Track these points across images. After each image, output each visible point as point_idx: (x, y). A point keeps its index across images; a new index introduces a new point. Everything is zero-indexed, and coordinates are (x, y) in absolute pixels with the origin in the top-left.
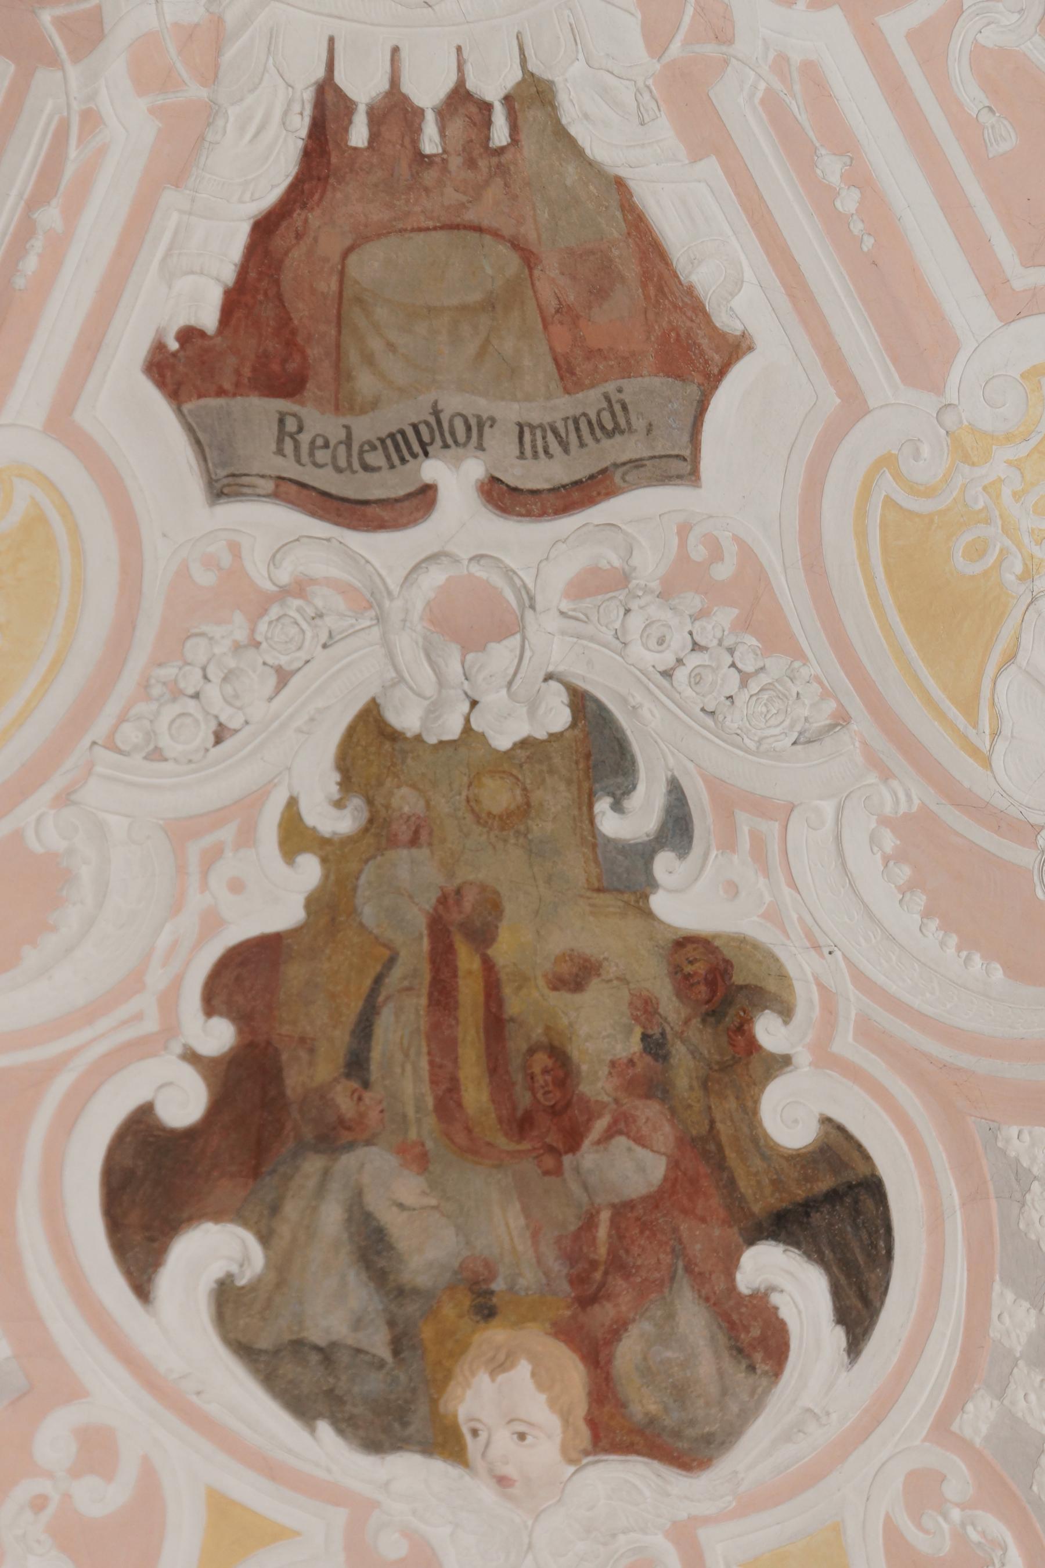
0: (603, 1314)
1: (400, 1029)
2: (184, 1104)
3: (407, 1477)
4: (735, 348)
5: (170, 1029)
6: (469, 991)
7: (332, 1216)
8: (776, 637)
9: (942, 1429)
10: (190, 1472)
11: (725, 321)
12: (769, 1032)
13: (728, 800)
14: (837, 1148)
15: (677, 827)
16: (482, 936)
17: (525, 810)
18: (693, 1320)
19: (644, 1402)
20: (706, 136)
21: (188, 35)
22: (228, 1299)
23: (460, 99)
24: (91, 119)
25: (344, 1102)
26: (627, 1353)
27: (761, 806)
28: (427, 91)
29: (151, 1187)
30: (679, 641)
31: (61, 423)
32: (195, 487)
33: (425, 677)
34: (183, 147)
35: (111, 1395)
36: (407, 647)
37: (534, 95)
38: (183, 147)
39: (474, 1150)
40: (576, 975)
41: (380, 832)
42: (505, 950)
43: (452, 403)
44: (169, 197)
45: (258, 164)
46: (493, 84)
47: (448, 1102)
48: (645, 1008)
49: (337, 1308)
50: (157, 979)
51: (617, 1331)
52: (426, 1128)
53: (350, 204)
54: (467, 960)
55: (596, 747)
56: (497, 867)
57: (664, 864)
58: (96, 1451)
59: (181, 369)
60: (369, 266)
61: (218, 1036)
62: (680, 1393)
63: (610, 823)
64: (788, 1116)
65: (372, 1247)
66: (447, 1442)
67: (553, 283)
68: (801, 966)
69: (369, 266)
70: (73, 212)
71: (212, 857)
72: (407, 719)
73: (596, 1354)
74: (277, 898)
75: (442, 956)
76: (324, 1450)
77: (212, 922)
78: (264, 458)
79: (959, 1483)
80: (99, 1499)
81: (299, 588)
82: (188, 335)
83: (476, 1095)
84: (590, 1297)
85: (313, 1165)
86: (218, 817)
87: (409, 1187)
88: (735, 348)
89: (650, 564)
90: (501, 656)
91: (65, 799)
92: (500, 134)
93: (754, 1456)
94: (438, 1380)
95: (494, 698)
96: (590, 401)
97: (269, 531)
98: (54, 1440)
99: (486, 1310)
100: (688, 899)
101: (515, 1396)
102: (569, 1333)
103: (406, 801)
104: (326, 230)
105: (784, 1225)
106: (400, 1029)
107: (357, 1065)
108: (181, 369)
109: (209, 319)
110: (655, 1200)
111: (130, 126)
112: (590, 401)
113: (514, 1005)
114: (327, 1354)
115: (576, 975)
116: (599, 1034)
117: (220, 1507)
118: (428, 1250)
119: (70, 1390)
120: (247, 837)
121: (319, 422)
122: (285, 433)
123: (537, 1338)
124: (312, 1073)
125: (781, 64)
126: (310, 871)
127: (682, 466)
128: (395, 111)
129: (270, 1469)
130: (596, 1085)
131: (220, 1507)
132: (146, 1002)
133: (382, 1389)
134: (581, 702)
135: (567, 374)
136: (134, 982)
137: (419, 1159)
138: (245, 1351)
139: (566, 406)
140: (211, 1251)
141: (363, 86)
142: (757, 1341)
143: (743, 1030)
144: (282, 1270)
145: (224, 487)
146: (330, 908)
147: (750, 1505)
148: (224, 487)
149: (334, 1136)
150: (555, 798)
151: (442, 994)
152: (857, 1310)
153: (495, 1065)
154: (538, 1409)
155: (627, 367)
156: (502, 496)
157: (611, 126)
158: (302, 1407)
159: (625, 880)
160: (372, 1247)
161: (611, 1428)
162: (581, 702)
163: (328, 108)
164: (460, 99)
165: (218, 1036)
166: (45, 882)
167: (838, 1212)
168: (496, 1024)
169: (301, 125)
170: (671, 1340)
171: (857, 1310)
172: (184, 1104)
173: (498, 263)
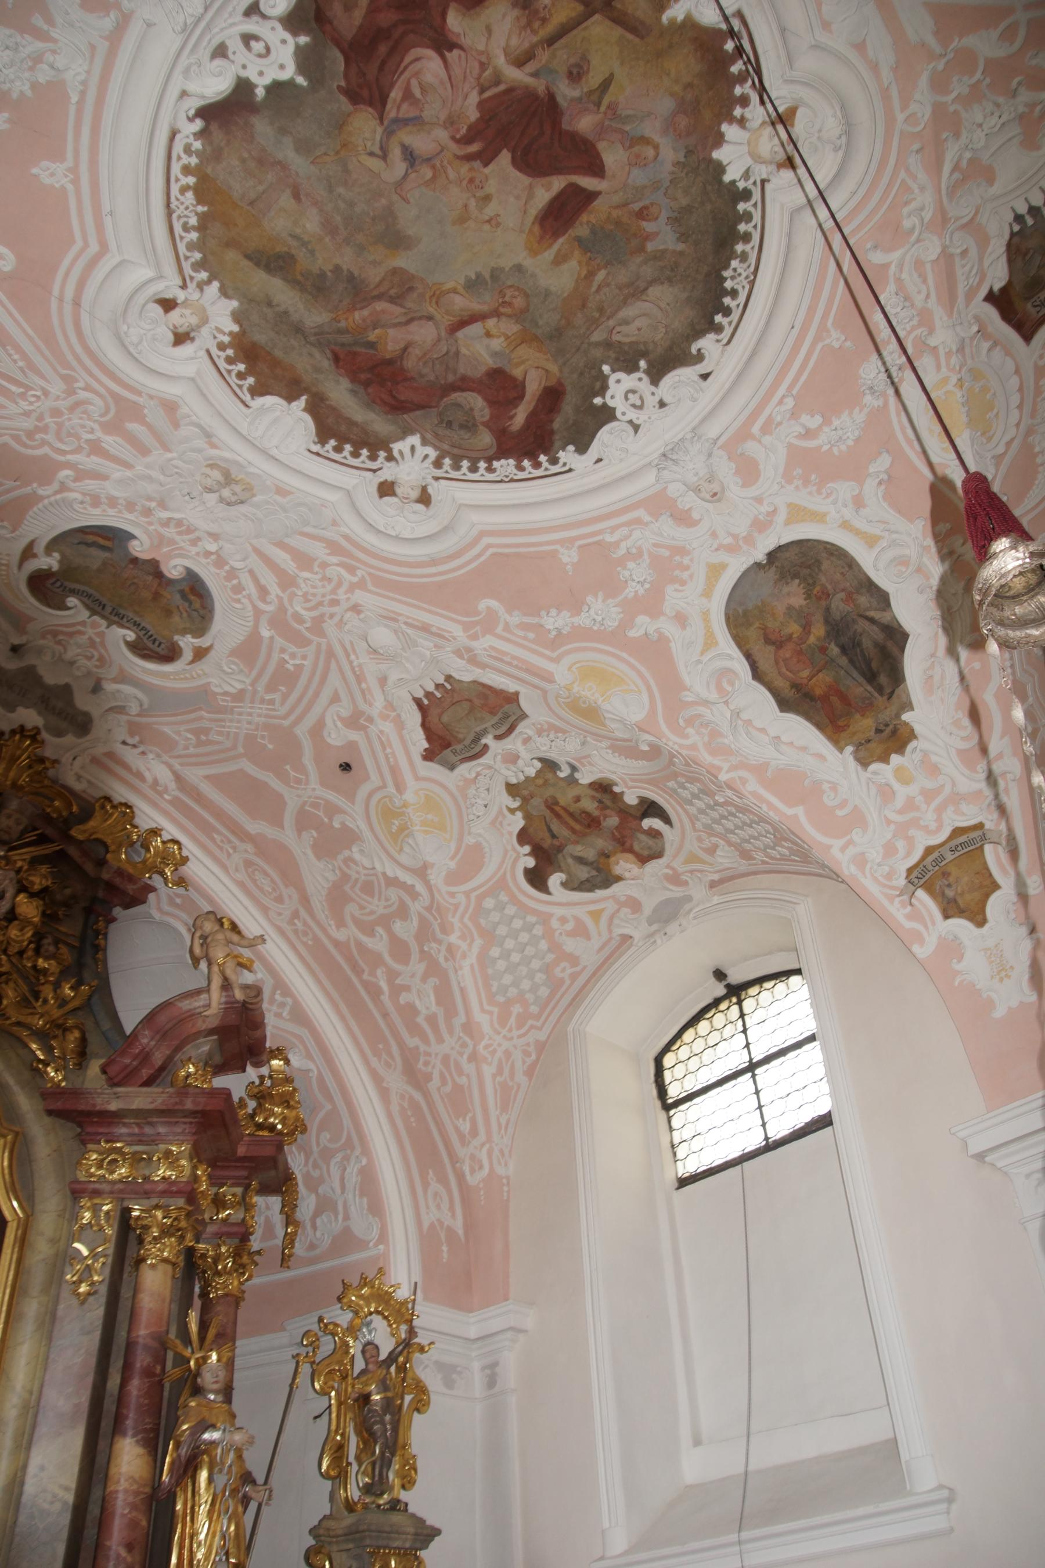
0: (627, 845)
1: (556, 826)
2: (531, 863)
3: (616, 889)
4: (517, 694)
5: (518, 853)
6: (562, 812)
7: (570, 861)
8: (564, 732)
9: (695, 830)
10: (580, 912)
11: (512, 690)
12: (616, 789)
13: (578, 760)
14: (643, 800)
15: (574, 769)
16: (557, 803)
17: (546, 781)
18: (643, 837)
19: (646, 853)
20: (484, 666)
21: (385, 707)
22: (564, 885)
23: (438, 686)
24: (381, 732)
25: (556, 843)
26: (636, 847)
27: (585, 757)
28: (431, 688)
29: (537, 878)
30: (548, 743)
31: (417, 778)
32: (447, 772)
33: (510, 773)
34: (400, 724)
35: (559, 911)
36: (504, 771)
37: (449, 678)
38: (400, 724)
39: (584, 835)
40: (578, 799)
41: (525, 800)
42: (562, 802)
43: (478, 729)
44: (405, 732)
45: (413, 718)
46: (441, 680)
47: (574, 831)
48: (593, 798)
49: (583, 873)
50: (509, 848)
51: (632, 846)
52: (574, 837)
53: (434, 713)
54: (557, 808)
55: (549, 765)
56: (550, 792)
57: (577, 775)
58: (563, 920)
59: (429, 756)
60: (445, 718)
61: (527, 849)
62: (649, 848)
63: (562, 775)
64: (631, 799)
65: (581, 860)
66: (619, 879)
67: (477, 702)
68: (613, 777)
69: (445, 718)
70: (391, 747)
71: (501, 823)
72: (514, 781)
73: (631, 851)
74: (518, 822)
75: (552, 810)
76: (600, 893)
77: (510, 833)
78: (455, 759)
79: (704, 835)
80: (570, 926)
81: (478, 774)
82: (426, 750)
83: (577, 827)
84: (623, 843)
85: (560, 856)
86: (496, 818)
87: (579, 848)
88: (517, 694)
89: (530, 733)
90: (520, 762)
91: (469, 834)
92: (449, 687)
93: (669, 851)
94: (609, 871)
95: (526, 769)
96: (500, 715)
97: (465, 770)
98: (555, 924)
99: (608, 856)
100: (585, 778)
101: (624, 865)
102: (624, 851)
103: (525, 793)
104: (433, 718)
105: (645, 815)
106: (556, 826)
107: (554, 836)
108: (429, 756)
109: (426, 745)
110: (621, 824)
111: (388, 727)
112: (500, 715)
113: (571, 810)
114: (587, 880)
115: (578, 799)
116: (589, 805)
117: (591, 913)
118: (590, 854)
119: (551, 915)
120: (504, 816)
121: (459, 747)
122: (455, 753)
123: (619, 855)
124: (547, 842)
125: (485, 649)
126: (519, 815)
127: (524, 716)
128: (428, 695)
129: (593, 902)
130: (596, 813)
131: (591, 913)
132: (511, 853)
133: (602, 877)
134: (540, 760)
135: (493, 712)
136: (506, 852)
137: (577, 843)
138: (573, 889)
139: (496, 719)
140: (555, 880)
141: (420, 694)
142: (655, 834)
143: (612, 792)
144: (569, 874)
145: (452, 768)
146: (527, 817)
147: (675, 857)
148: (452, 768)
149: (560, 849)
150: (549, 776)
151: (558, 816)
152: (667, 821)
153: (576, 820)
154: (629, 866)
155: (502, 707)
156: (498, 738)
157: (466, 673)
158: (590, 890)
159: (571, 780)
160: (581, 860)
161: (643, 860)
162: (540, 760)
163: (418, 702)
164: (438, 686)
165: (527, 849)
166: (478, 848)
167: (650, 808)
168: (571, 815)
169: (415, 707)
170: (641, 843)
171: (667, 821)
172: (531, 863)
173: (466, 705)
